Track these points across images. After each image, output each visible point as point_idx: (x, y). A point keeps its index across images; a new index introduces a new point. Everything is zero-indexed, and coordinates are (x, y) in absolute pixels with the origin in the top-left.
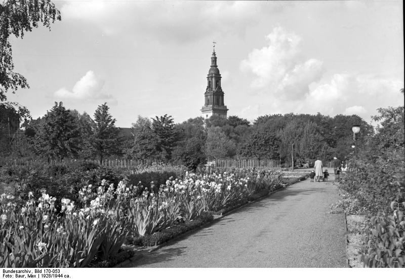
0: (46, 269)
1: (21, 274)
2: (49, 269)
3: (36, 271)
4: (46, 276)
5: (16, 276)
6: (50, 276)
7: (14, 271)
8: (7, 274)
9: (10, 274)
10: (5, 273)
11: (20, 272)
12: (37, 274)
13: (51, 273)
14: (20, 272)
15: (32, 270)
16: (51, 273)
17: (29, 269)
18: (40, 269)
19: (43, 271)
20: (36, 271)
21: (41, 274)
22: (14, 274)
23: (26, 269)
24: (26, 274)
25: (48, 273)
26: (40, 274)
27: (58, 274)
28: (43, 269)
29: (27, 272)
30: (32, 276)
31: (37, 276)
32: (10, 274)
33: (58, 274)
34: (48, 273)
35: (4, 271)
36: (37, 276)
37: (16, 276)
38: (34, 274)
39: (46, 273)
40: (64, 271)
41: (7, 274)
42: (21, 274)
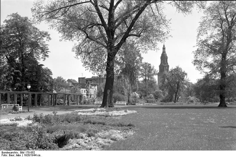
0: (27, 151)
1: (13, 154)
2: (28, 151)
3: (21, 153)
4: (27, 155)
5: (10, 155)
6: (29, 155)
7: (8, 153)
8: (4, 154)
9: (6, 154)
10: (3, 154)
11: (12, 153)
12: (22, 154)
13: (30, 154)
14: (12, 153)
15: (19, 152)
16: (30, 154)
17: (17, 151)
18: (23, 151)
19: (25, 153)
20: (21, 153)
21: (24, 154)
22: (8, 154)
23: (15, 151)
24: (15, 154)
25: (28, 154)
26: (24, 154)
27: (34, 154)
28: (25, 151)
29: (16, 153)
30: (19, 155)
31: (22, 155)
32: (6, 154)
33: (34, 154)
34: (28, 154)
35: (2, 152)
36: (22, 155)
37: (10, 155)
38: (20, 154)
39: (27, 154)
40: (37, 152)
41: (4, 154)
42: (13, 154)
